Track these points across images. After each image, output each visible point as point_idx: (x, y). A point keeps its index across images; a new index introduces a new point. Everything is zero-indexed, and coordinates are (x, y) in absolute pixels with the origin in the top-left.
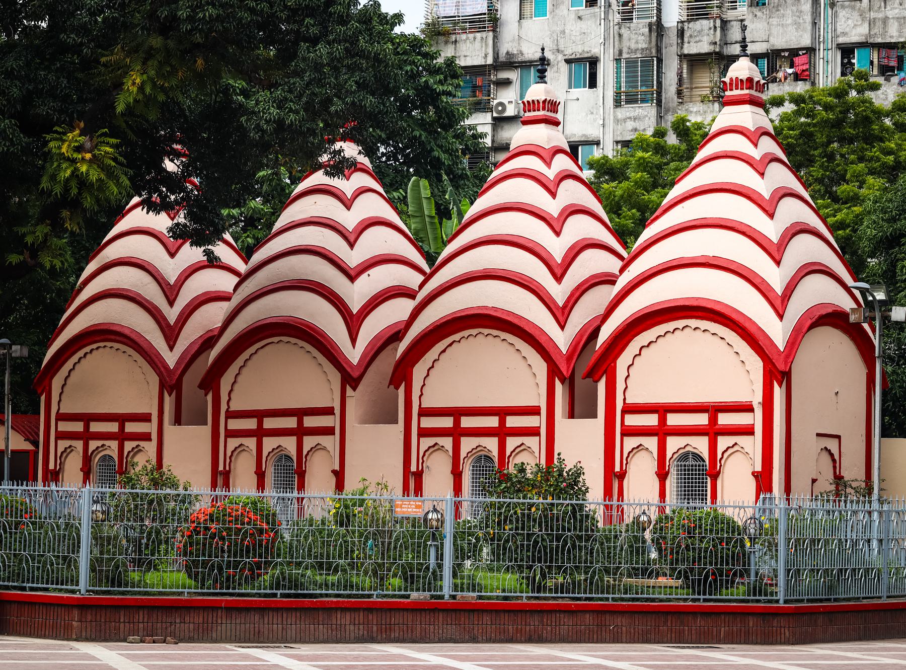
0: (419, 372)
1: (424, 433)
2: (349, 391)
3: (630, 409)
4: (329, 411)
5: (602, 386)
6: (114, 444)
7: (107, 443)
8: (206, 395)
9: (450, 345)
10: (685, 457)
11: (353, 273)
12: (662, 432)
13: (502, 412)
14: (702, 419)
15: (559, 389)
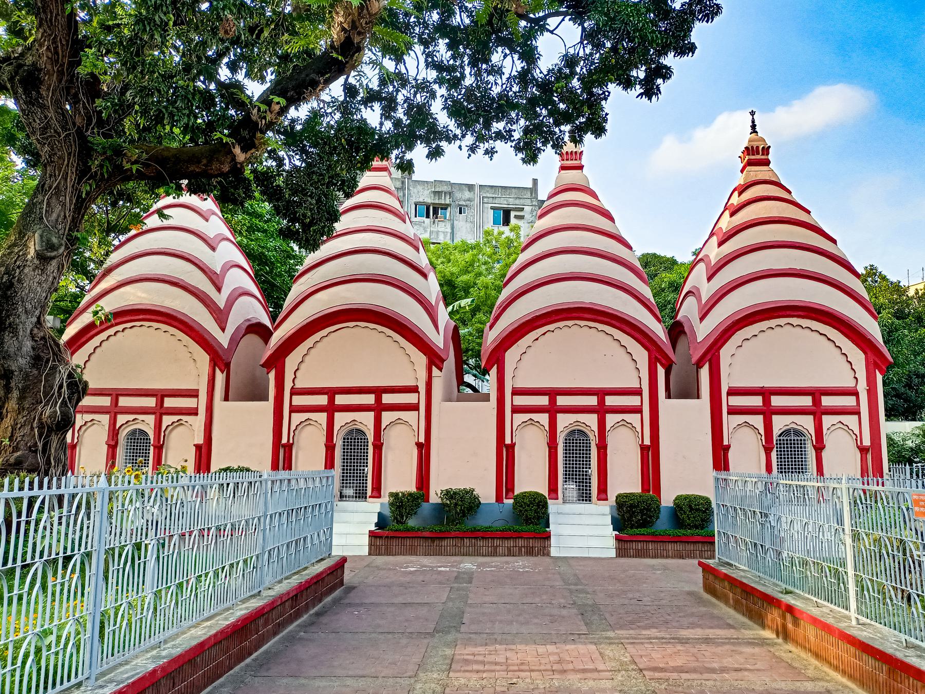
0: (511, 356)
1: (516, 410)
2: (435, 371)
3: (732, 392)
4: (414, 390)
5: (705, 373)
6: (151, 419)
7: (141, 417)
8: (268, 373)
9: (544, 334)
10: (786, 433)
11: (425, 271)
12: (768, 412)
13: (602, 393)
14: (806, 401)
15: (661, 372)
